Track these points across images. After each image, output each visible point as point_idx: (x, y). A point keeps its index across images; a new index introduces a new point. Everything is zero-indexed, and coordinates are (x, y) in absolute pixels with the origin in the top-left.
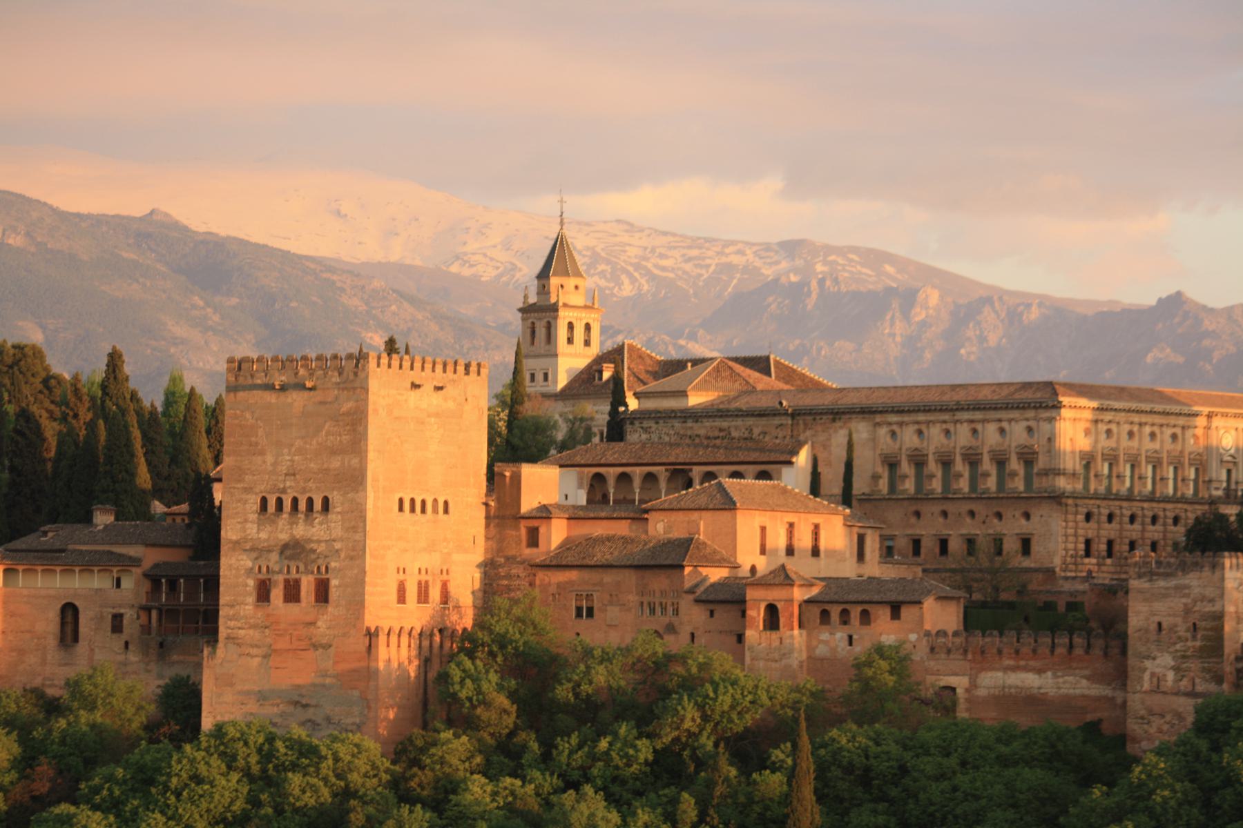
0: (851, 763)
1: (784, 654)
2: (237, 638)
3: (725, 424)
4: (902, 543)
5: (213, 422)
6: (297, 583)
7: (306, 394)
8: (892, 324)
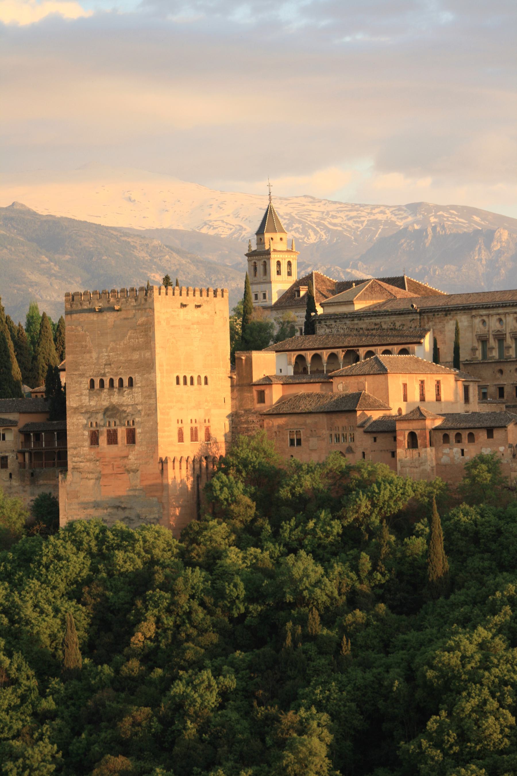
0: (466, 529)
1: (422, 463)
2: (79, 468)
3: (378, 321)
4: (492, 390)
5: (58, 334)
6: (115, 432)
7: (115, 314)
8: (480, 253)
